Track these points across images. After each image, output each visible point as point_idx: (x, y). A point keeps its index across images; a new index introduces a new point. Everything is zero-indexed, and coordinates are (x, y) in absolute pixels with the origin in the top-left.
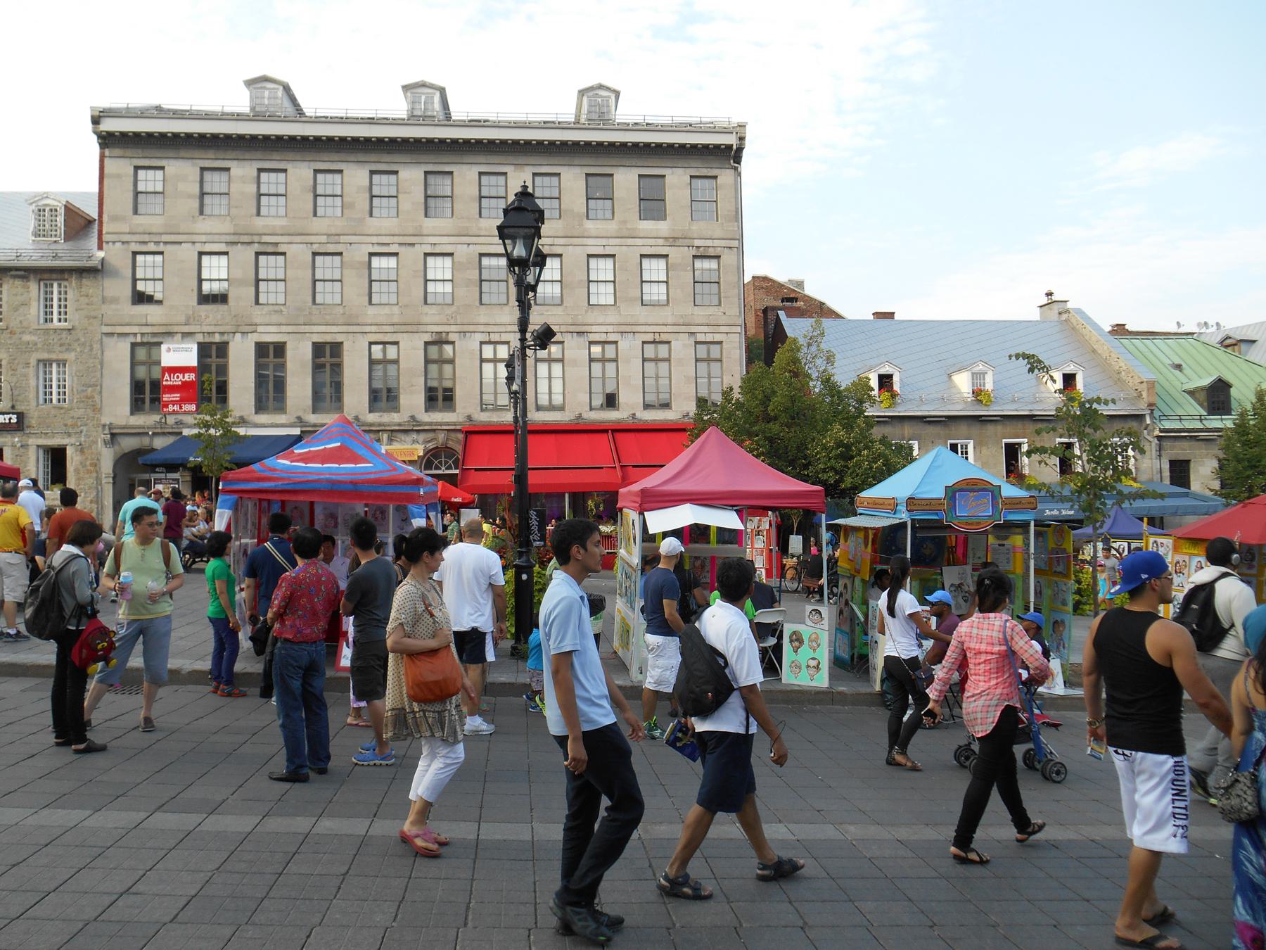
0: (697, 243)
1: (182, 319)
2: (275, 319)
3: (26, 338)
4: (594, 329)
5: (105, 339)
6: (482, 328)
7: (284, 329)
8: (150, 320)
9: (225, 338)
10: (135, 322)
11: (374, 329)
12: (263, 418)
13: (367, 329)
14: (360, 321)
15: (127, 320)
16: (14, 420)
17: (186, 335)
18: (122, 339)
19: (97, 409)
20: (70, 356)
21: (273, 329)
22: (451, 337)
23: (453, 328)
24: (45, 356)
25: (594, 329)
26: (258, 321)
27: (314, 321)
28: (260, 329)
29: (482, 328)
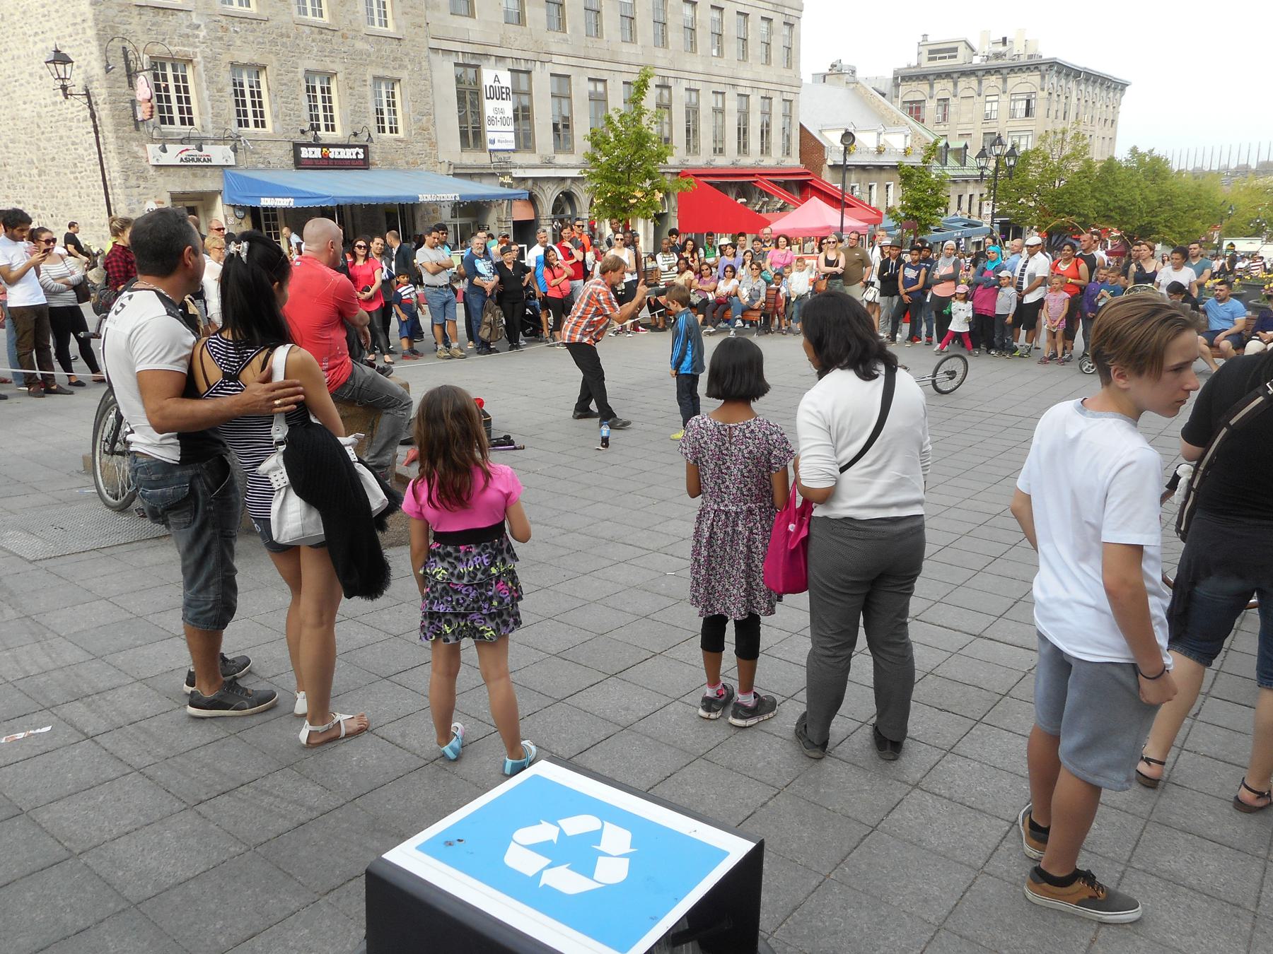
0: (787, 11)
1: (497, 42)
2: (565, 49)
3: (360, 45)
4: (742, 82)
5: (432, 56)
6: (686, 75)
7: (573, 61)
8: (473, 37)
9: (529, 66)
10: (459, 37)
11: (624, 68)
12: (561, 159)
13: (624, 68)
14: (619, 59)
15: (452, 35)
16: (361, 156)
17: (500, 58)
18: (446, 57)
19: (433, 145)
20: (404, 75)
21: (562, 60)
22: (671, 82)
23: (672, 73)
24: (380, 72)
25: (742, 82)
26: (553, 49)
27: (593, 56)
28: (555, 59)
29: (686, 75)
